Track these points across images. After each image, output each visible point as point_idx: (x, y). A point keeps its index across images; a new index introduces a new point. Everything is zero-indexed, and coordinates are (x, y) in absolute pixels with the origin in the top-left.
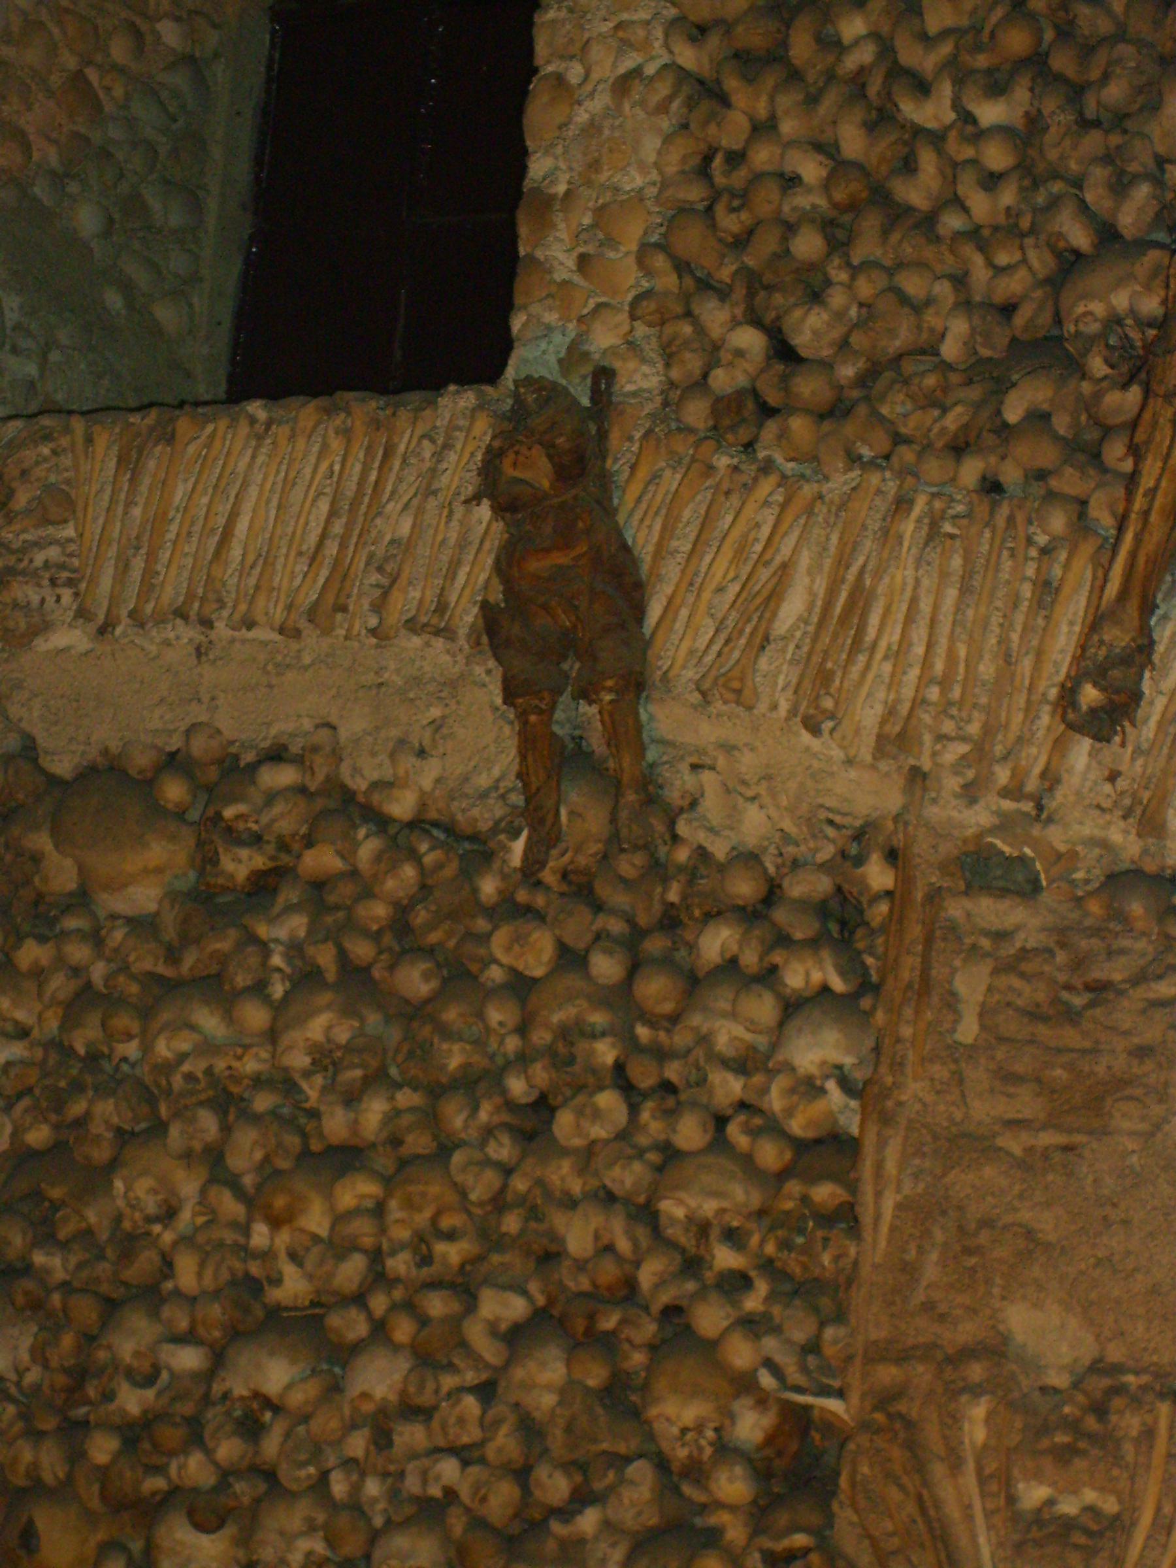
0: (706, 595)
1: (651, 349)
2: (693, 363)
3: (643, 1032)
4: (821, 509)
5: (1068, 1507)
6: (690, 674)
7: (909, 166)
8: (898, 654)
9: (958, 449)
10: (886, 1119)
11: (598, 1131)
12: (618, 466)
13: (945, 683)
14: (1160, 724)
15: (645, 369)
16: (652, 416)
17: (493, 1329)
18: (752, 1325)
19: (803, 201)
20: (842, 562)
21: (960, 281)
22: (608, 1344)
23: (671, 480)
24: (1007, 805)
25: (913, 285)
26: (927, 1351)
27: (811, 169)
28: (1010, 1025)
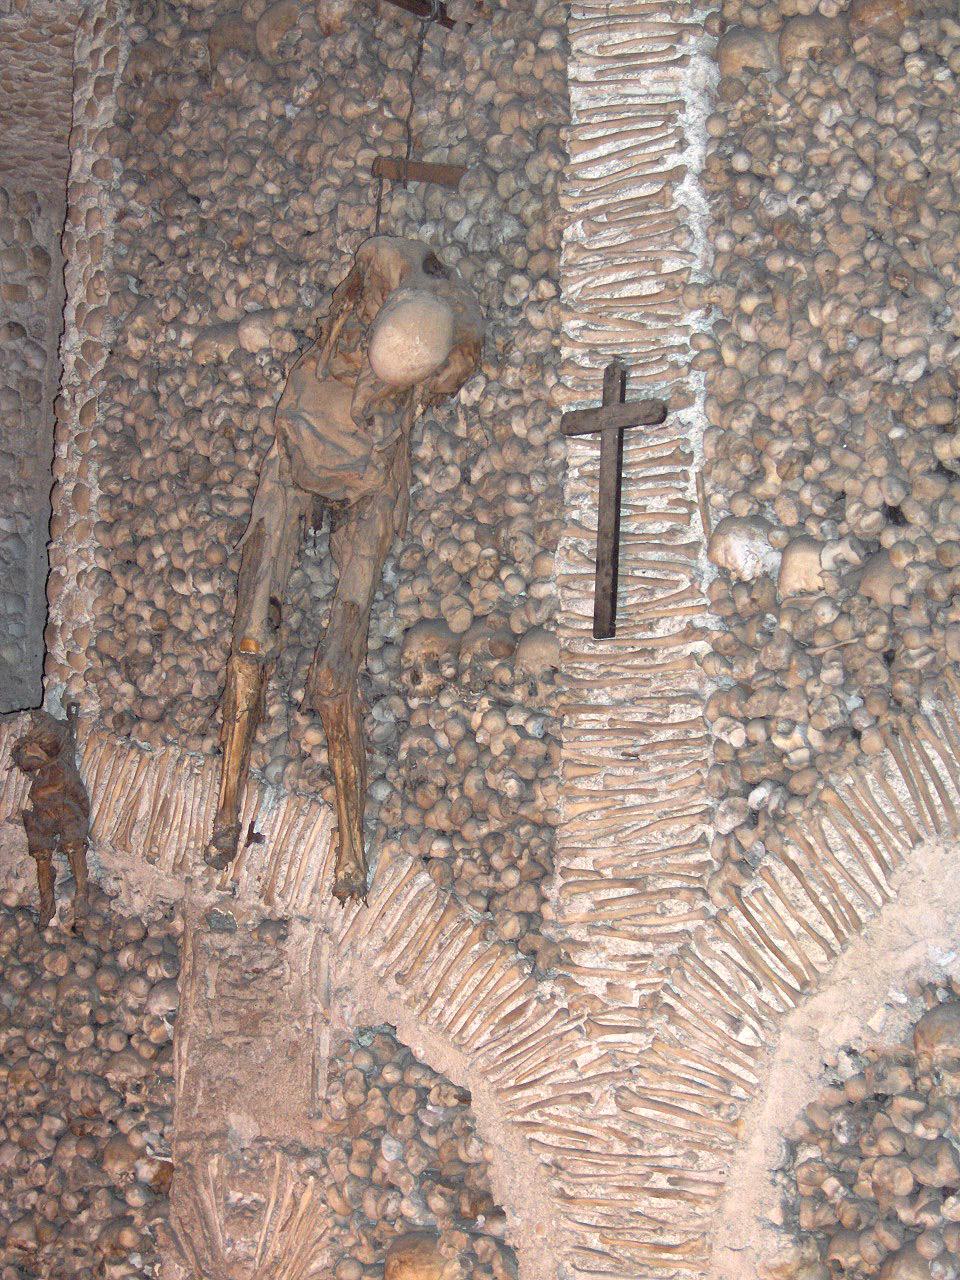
1: (95, 693)
2: (109, 698)
5: (247, 1201)
7: (179, 614)
8: (181, 827)
9: (203, 734)
10: (181, 1034)
11: (82, 1044)
12: (82, 747)
13: (196, 840)
16: (94, 724)
17: (48, 1135)
18: (142, 1128)
19: (143, 628)
20: (159, 787)
21: (199, 661)
22: (92, 1139)
23: (100, 752)
25: (185, 663)
26: (198, 1136)
27: (146, 613)
28: (226, 991)
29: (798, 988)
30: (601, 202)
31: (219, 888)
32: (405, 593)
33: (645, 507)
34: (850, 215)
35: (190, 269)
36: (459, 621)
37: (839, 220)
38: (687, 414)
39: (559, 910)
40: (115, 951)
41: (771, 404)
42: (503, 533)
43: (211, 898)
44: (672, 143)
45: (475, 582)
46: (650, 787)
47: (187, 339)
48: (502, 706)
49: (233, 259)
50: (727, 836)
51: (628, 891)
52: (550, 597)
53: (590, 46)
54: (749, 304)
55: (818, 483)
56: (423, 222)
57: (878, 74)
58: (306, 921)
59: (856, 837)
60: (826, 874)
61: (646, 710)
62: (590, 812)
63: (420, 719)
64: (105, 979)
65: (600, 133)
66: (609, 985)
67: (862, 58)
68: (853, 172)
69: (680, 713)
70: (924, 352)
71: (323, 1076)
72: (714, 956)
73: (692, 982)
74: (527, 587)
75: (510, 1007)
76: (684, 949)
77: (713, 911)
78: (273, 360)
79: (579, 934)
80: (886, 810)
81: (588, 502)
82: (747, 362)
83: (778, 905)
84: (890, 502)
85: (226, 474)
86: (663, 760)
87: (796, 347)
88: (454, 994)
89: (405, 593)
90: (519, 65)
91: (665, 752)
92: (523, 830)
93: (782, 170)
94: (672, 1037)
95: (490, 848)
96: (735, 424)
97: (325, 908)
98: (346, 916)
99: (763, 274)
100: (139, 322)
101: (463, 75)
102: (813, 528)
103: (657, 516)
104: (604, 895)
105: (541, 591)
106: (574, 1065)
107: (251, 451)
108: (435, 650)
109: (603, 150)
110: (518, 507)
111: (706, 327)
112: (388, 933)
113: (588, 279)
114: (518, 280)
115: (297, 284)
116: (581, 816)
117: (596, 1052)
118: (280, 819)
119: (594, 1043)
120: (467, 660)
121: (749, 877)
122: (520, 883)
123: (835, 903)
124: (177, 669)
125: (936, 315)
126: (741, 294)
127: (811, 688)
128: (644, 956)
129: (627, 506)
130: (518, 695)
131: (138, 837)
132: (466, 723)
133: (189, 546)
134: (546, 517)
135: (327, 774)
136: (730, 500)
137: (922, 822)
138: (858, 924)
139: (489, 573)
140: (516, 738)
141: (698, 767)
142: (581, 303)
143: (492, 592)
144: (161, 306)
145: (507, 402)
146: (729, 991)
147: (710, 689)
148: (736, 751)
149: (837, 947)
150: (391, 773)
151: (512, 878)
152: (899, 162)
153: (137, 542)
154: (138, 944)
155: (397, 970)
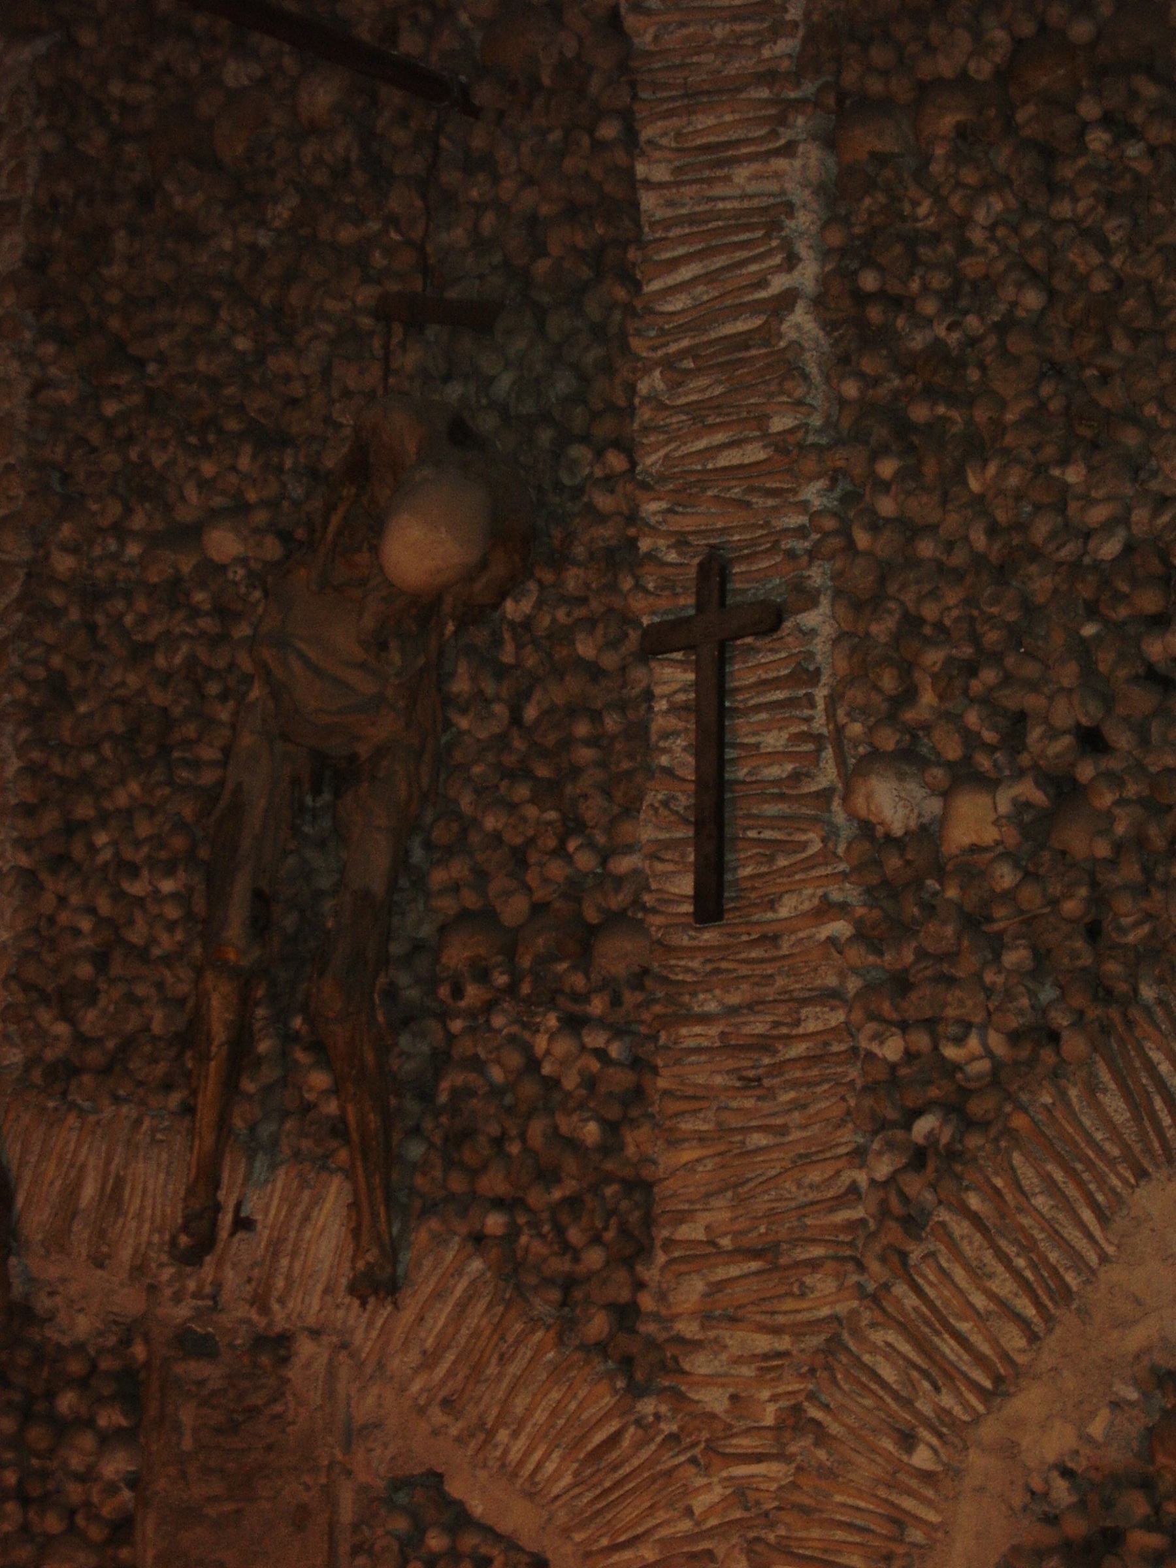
0: (45, 1188)
3: (35, 1462)
4: (99, 1131)
6: (40, 1237)
7: (131, 922)
8: (139, 1216)
9: (167, 1086)
13: (160, 1231)
14: (267, 1247)
15: (15, 1050)
19: (83, 943)
20: (108, 1163)
21: (160, 986)
23: (26, 1118)
24: (200, 1303)
25: (141, 990)
27: (86, 924)
29: (988, 1384)
30: (685, 343)
31: (197, 1295)
32: (439, 877)
33: (757, 746)
34: (1018, 343)
35: (133, 455)
36: (514, 910)
37: (1002, 351)
38: (810, 619)
39: (662, 1297)
40: (50, 1395)
41: (921, 599)
42: (569, 789)
43: (183, 1312)
44: (778, 260)
45: (533, 857)
46: (779, 1121)
47: (133, 550)
48: (574, 1023)
49: (193, 440)
50: (885, 1184)
51: (754, 1265)
52: (636, 872)
53: (665, 134)
54: (887, 468)
55: (986, 701)
56: (447, 378)
57: (1049, 153)
58: (315, 1333)
59: (1059, 1176)
60: (1022, 1228)
61: (769, 1018)
62: (698, 1160)
63: (465, 1047)
64: (38, 1435)
65: (681, 251)
66: (734, 1398)
67: (1027, 132)
68: (1020, 286)
69: (815, 1020)
70: (1123, 519)
71: (344, 1548)
72: (874, 1349)
73: (846, 1387)
74: (604, 862)
75: (599, 1437)
76: (835, 1339)
77: (871, 1287)
78: (251, 574)
79: (689, 1329)
80: (1099, 1136)
81: (681, 742)
82: (885, 545)
83: (959, 1275)
84: (1084, 721)
85: (190, 730)
86: (794, 1084)
87: (953, 520)
88: (521, 1423)
89: (439, 877)
90: (569, 164)
91: (798, 1074)
92: (609, 1191)
93: (925, 288)
94: (821, 1466)
95: (565, 1218)
96: (874, 629)
97: (341, 1314)
98: (370, 1324)
99: (903, 428)
100: (66, 530)
101: (496, 179)
102: (984, 762)
103: (775, 757)
104: (721, 1273)
105: (623, 864)
106: (689, 1512)
107: (224, 697)
108: (482, 951)
109: (686, 273)
110: (586, 754)
111: (831, 503)
112: (430, 1343)
113: (673, 446)
114: (578, 451)
115: (280, 469)
116: (690, 1166)
117: (717, 1493)
118: (277, 1194)
119: (715, 1480)
120: (526, 962)
121: (919, 1239)
122: (607, 1263)
123: (1034, 1266)
124: (132, 999)
125: (1137, 470)
126: (875, 456)
127: (989, 977)
128: (779, 1355)
129: (734, 746)
130: (597, 1006)
131: (81, 1232)
132: (527, 1049)
133: (144, 829)
134: (626, 765)
135: (338, 1129)
136: (871, 730)
137: (1148, 1150)
138: (1065, 1294)
139: (552, 843)
140: (595, 1065)
141: (842, 1090)
142: (662, 478)
143: (557, 870)
144: (95, 507)
145: (568, 615)
146: (896, 1396)
147: (853, 985)
148: (893, 1067)
149: (1039, 1326)
150: (428, 1124)
151: (594, 1258)
152: (1082, 268)
153: (71, 828)
154: (83, 1383)
155: (443, 1393)
